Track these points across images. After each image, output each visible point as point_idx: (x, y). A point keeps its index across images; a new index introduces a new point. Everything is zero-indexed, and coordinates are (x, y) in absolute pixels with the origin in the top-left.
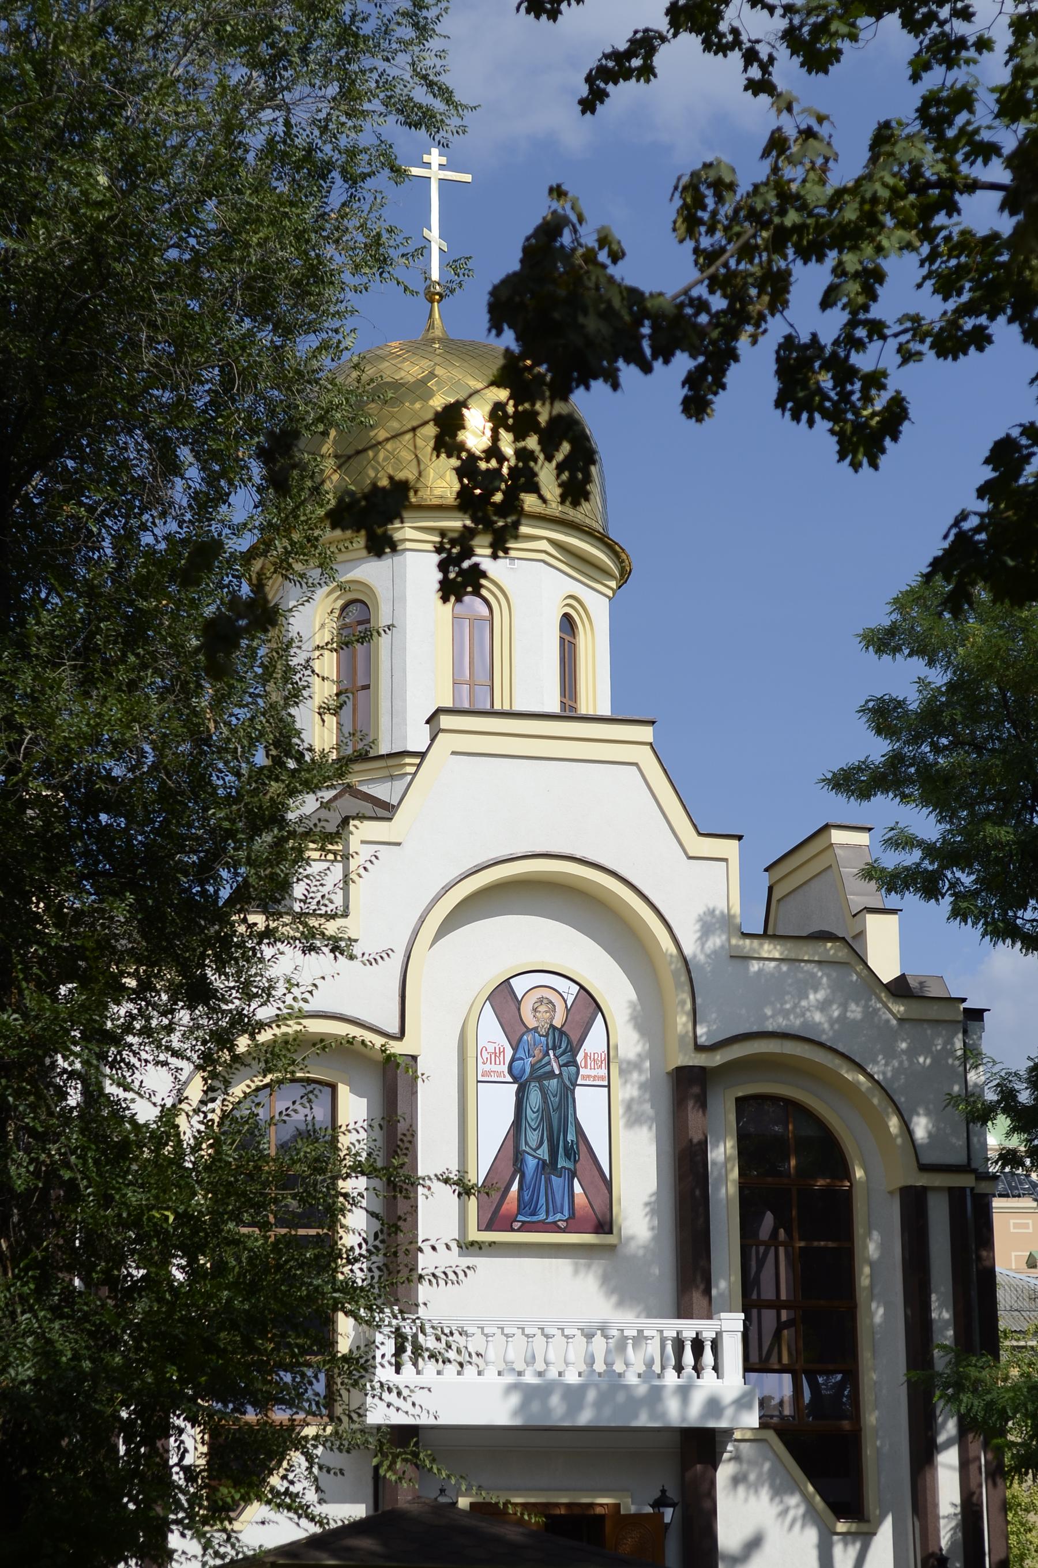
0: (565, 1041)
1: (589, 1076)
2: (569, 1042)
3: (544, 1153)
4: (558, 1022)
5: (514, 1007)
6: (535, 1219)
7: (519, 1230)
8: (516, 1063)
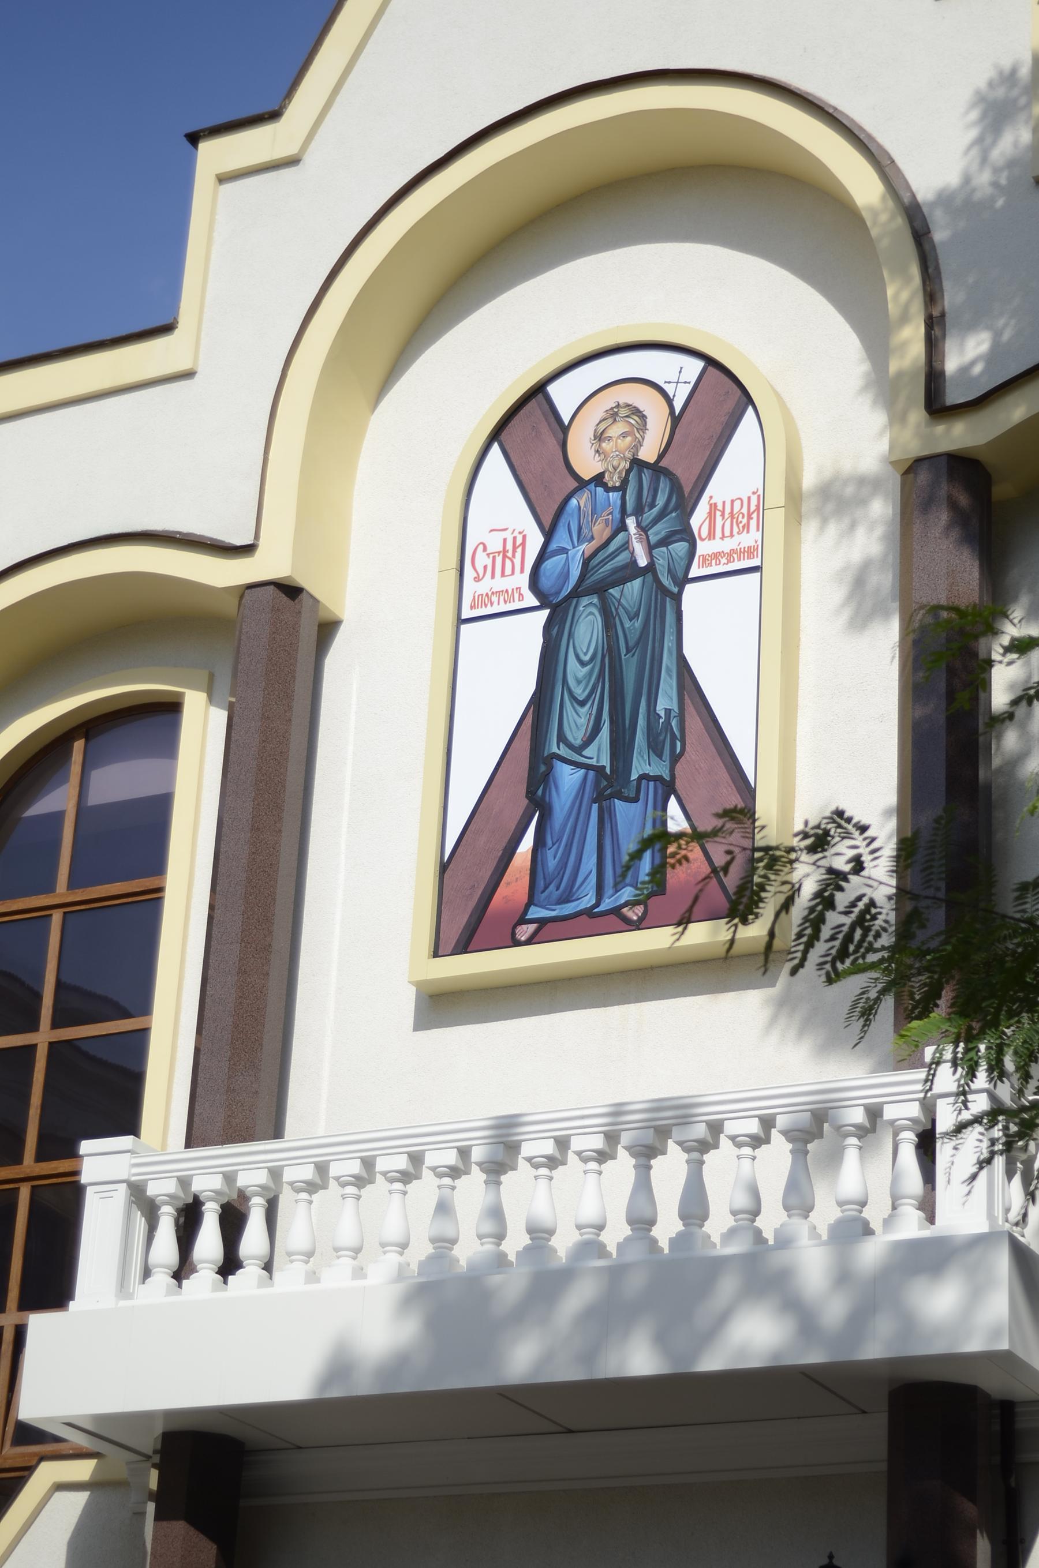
0: (667, 488)
1: (716, 556)
2: (676, 486)
3: (599, 753)
4: (648, 453)
5: (552, 444)
6: (569, 909)
7: (529, 942)
8: (548, 564)
